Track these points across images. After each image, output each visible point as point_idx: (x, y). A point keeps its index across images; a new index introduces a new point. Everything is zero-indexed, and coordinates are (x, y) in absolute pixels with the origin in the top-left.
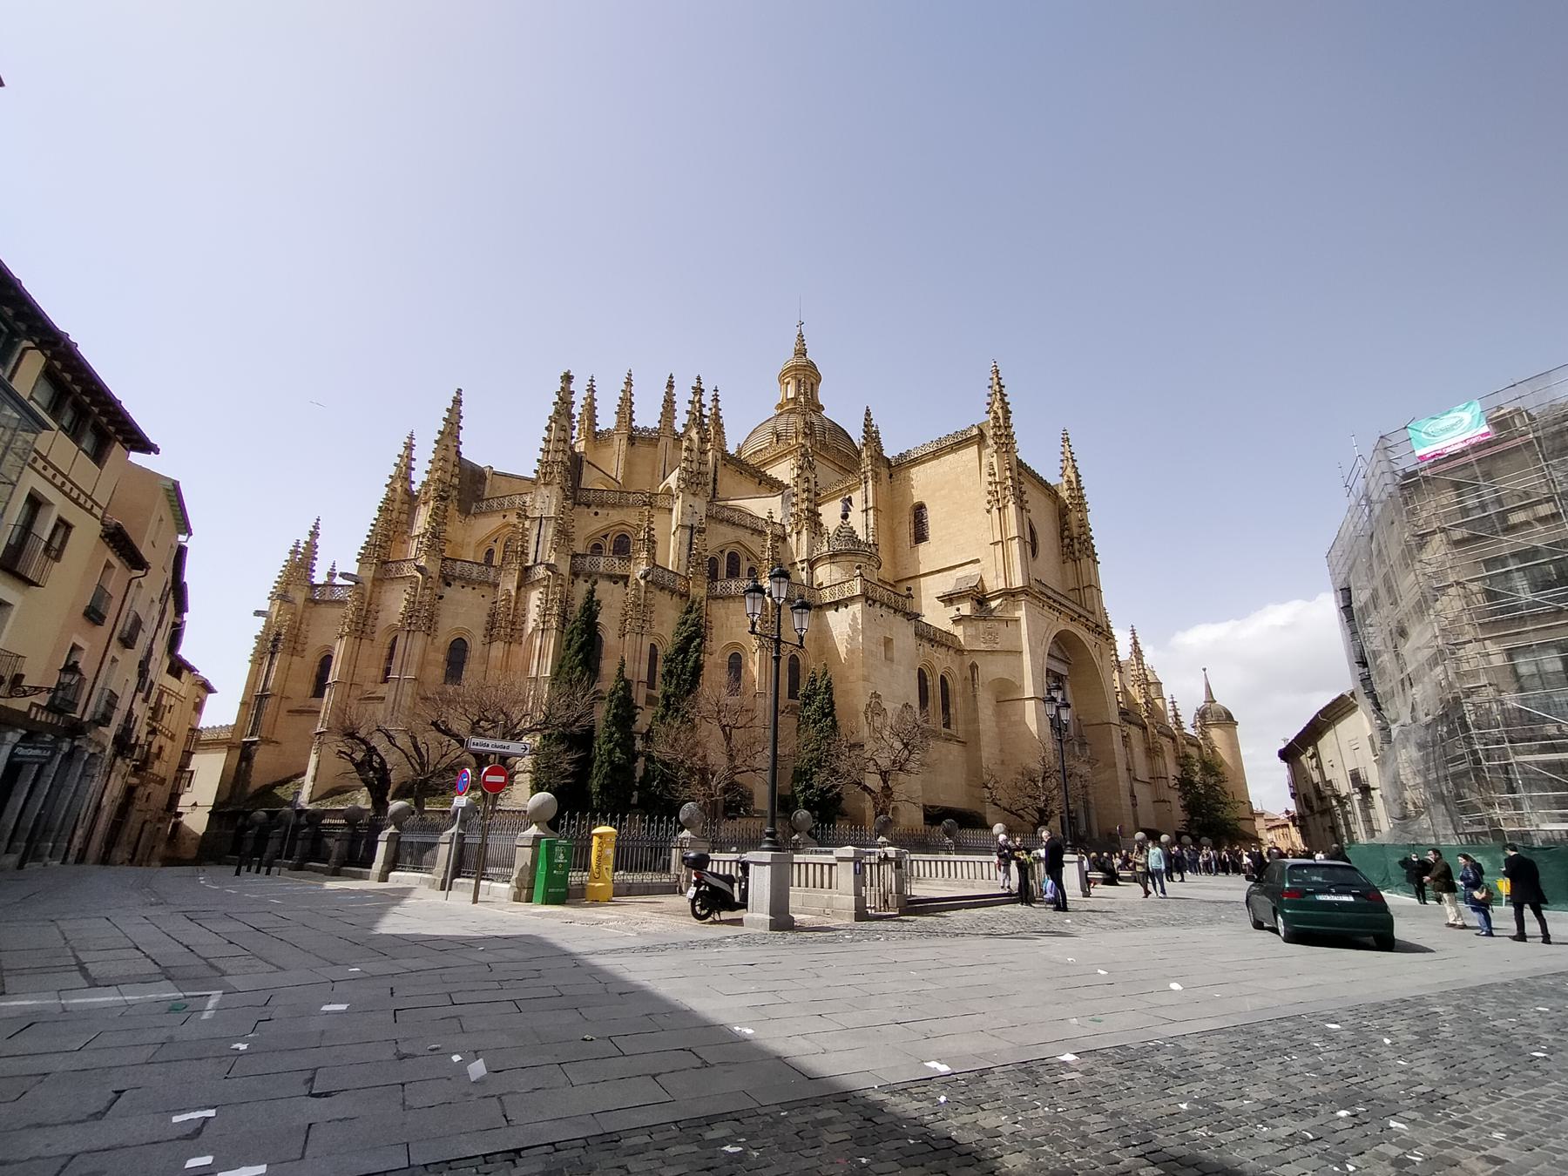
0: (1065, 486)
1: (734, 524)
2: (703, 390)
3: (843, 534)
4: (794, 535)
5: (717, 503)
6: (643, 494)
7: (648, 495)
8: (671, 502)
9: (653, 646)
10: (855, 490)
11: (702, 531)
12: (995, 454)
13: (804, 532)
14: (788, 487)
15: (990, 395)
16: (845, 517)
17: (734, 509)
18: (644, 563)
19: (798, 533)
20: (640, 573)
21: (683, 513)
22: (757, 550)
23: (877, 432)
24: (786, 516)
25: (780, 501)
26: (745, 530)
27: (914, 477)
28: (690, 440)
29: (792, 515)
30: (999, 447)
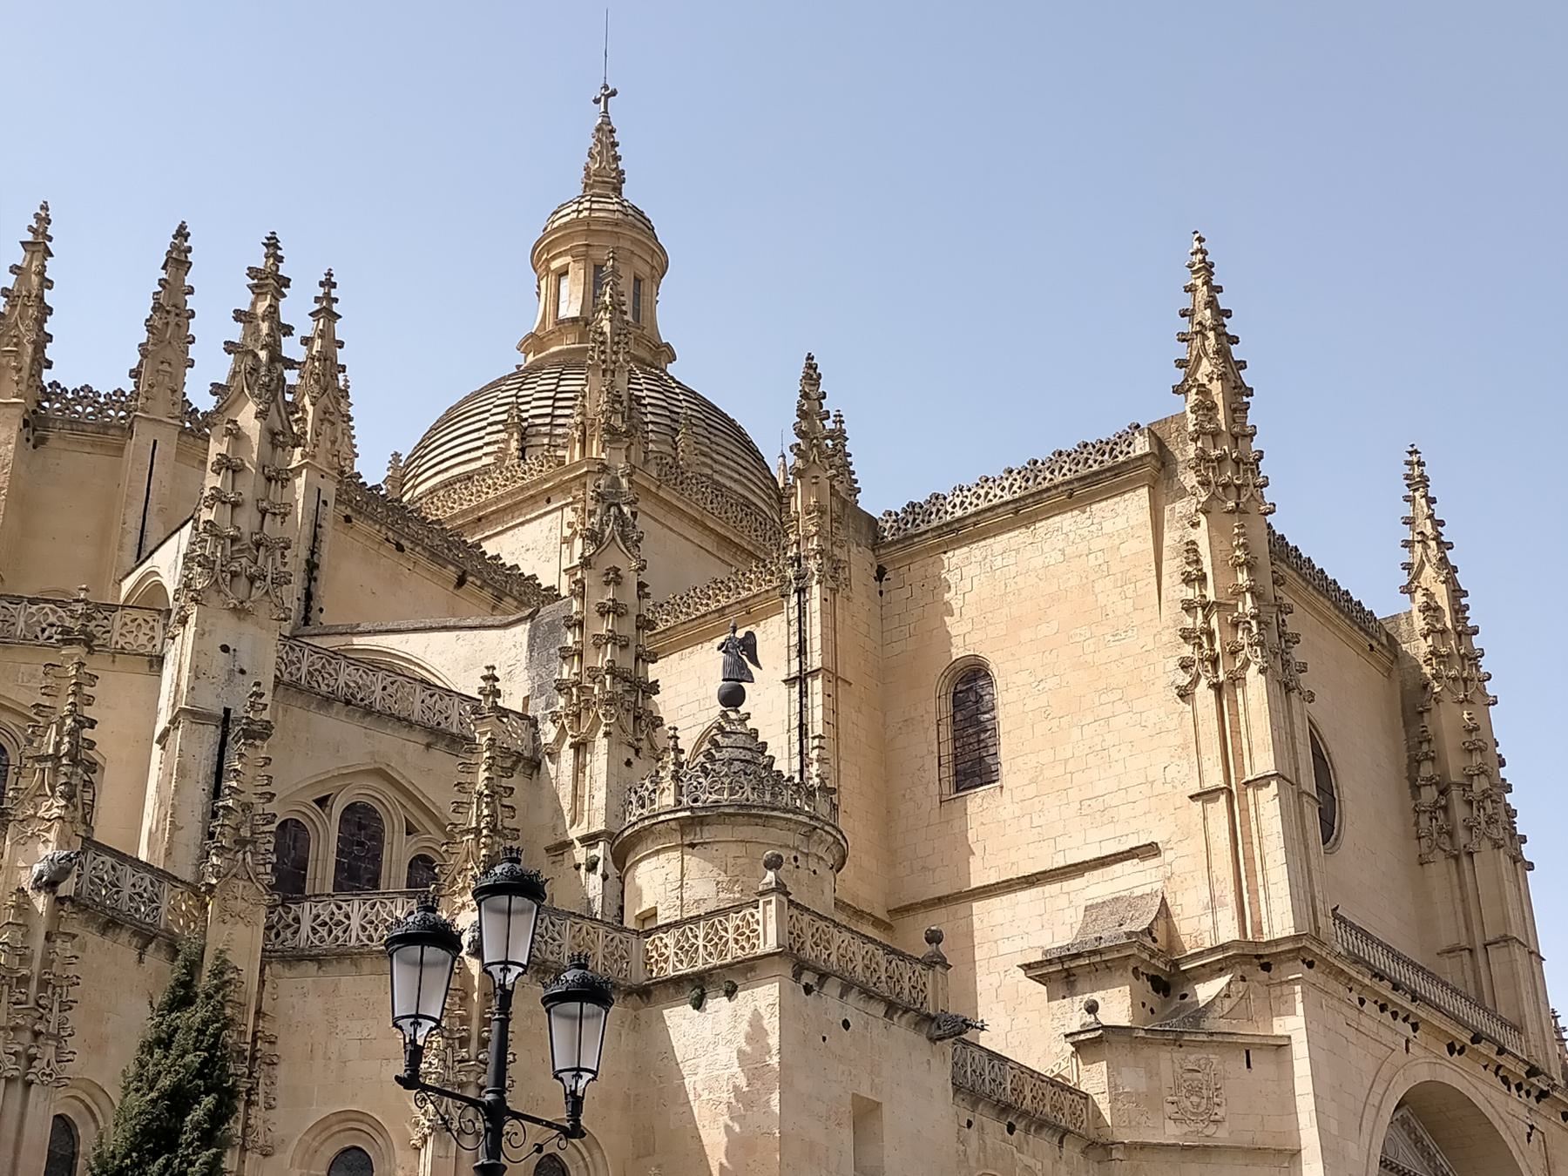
0: (1420, 623)
1: (368, 711)
2: (286, 282)
3: (725, 754)
4: (567, 754)
5: (316, 641)
6: (62, 604)
7: (79, 608)
8: (159, 633)
9: (63, 1127)
10: (767, 614)
11: (258, 733)
12: (1202, 518)
13: (601, 743)
14: (552, 595)
15: (1183, 338)
16: (732, 697)
17: (375, 663)
18: (52, 836)
19: (580, 747)
20: (37, 868)
21: (196, 672)
22: (440, 798)
23: (839, 436)
24: (540, 690)
25: (525, 639)
26: (404, 733)
27: (952, 579)
28: (236, 435)
29: (561, 687)
30: (1213, 497)
